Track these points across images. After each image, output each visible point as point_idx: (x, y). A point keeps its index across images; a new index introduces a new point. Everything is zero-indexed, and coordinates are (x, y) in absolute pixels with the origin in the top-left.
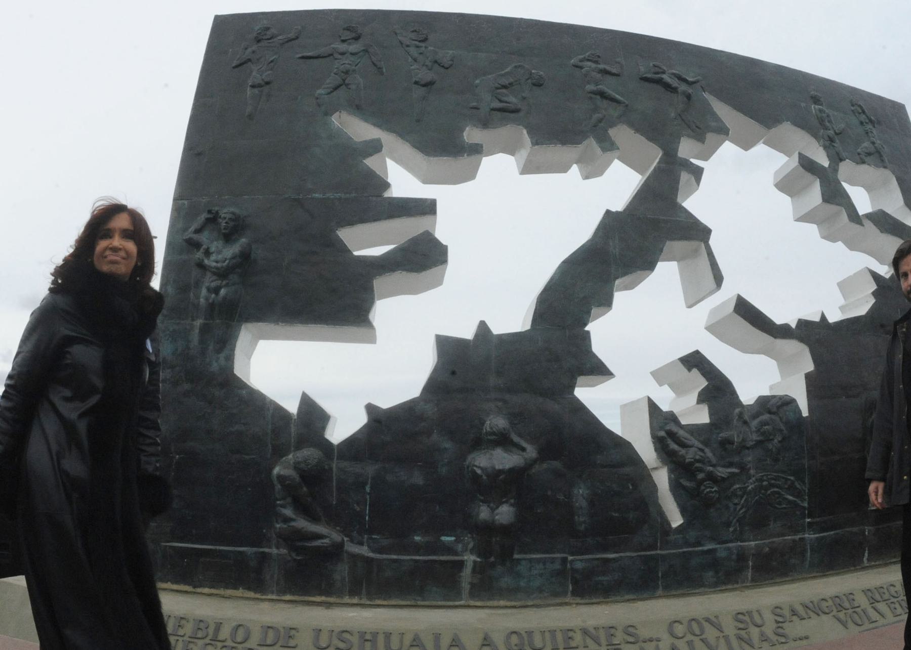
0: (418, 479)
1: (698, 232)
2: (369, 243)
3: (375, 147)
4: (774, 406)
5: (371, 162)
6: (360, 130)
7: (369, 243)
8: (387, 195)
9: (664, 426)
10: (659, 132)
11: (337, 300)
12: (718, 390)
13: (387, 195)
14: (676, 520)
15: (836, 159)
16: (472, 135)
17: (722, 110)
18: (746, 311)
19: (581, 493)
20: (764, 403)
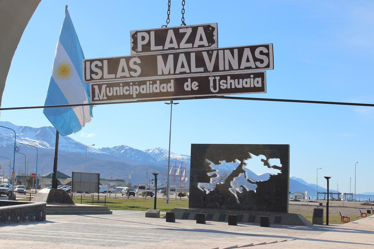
0: (214, 197)
1: (244, 172)
2: (209, 174)
3: (210, 164)
4: (251, 192)
5: (210, 165)
6: (209, 161)
7: (209, 174)
8: (211, 169)
9: (238, 193)
10: (241, 160)
11: (206, 180)
12: (244, 189)
13: (211, 169)
14: (238, 202)
15: (268, 159)
16: (220, 162)
17: (252, 155)
18: (249, 181)
19: (229, 199)
20: (250, 191)
